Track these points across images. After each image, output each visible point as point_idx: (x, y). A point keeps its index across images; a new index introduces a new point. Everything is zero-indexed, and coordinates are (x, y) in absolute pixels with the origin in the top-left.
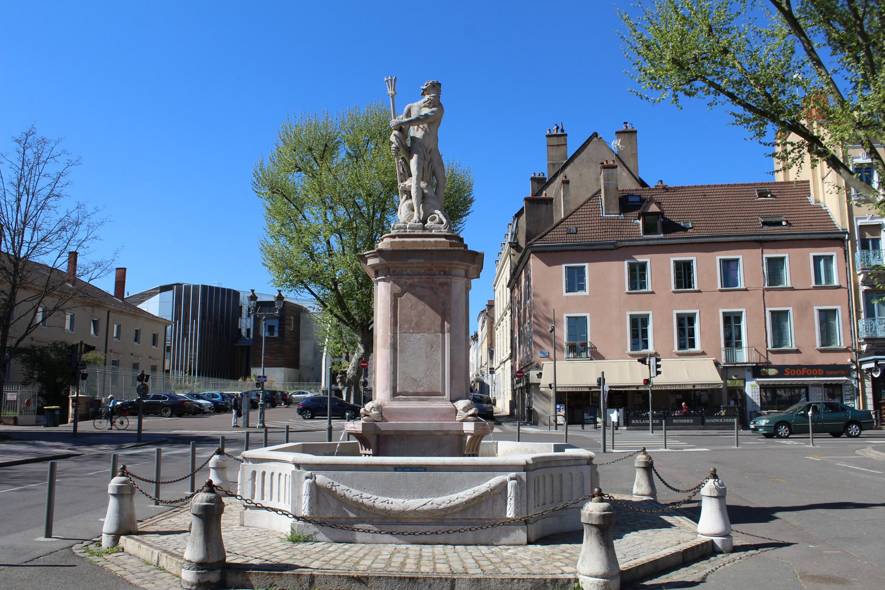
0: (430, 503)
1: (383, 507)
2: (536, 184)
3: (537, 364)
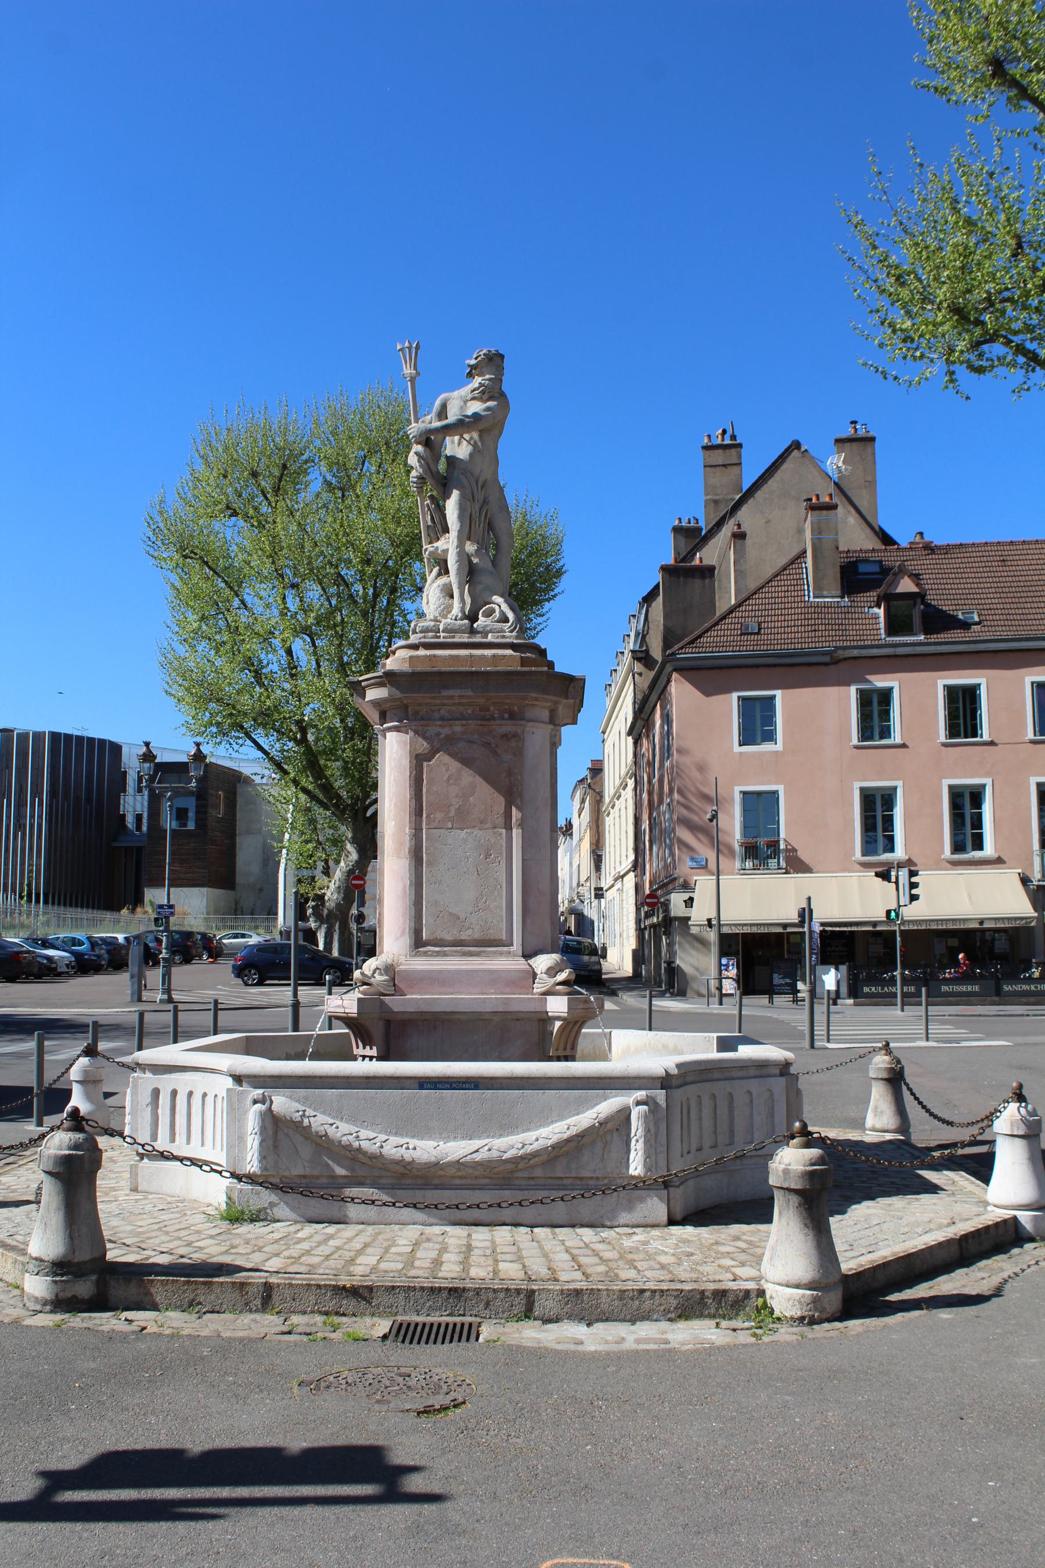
0: (486, 1148)
1: (398, 1156)
2: (682, 541)
3: (685, 880)
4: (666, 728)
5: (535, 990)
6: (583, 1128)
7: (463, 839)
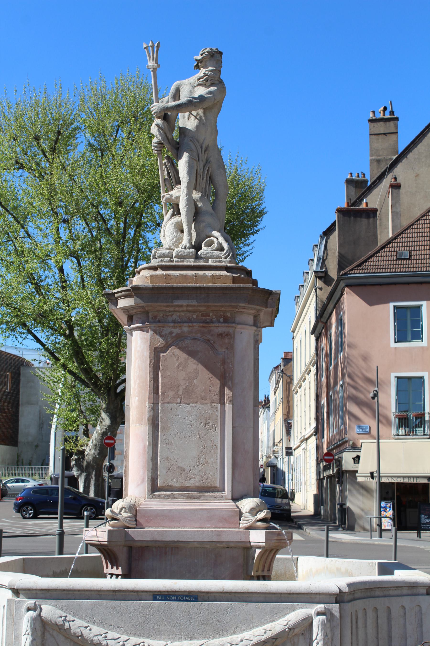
2: (353, 190)
3: (353, 443)
4: (340, 329)
5: (241, 525)
6: (276, 632)
7: (188, 411)
